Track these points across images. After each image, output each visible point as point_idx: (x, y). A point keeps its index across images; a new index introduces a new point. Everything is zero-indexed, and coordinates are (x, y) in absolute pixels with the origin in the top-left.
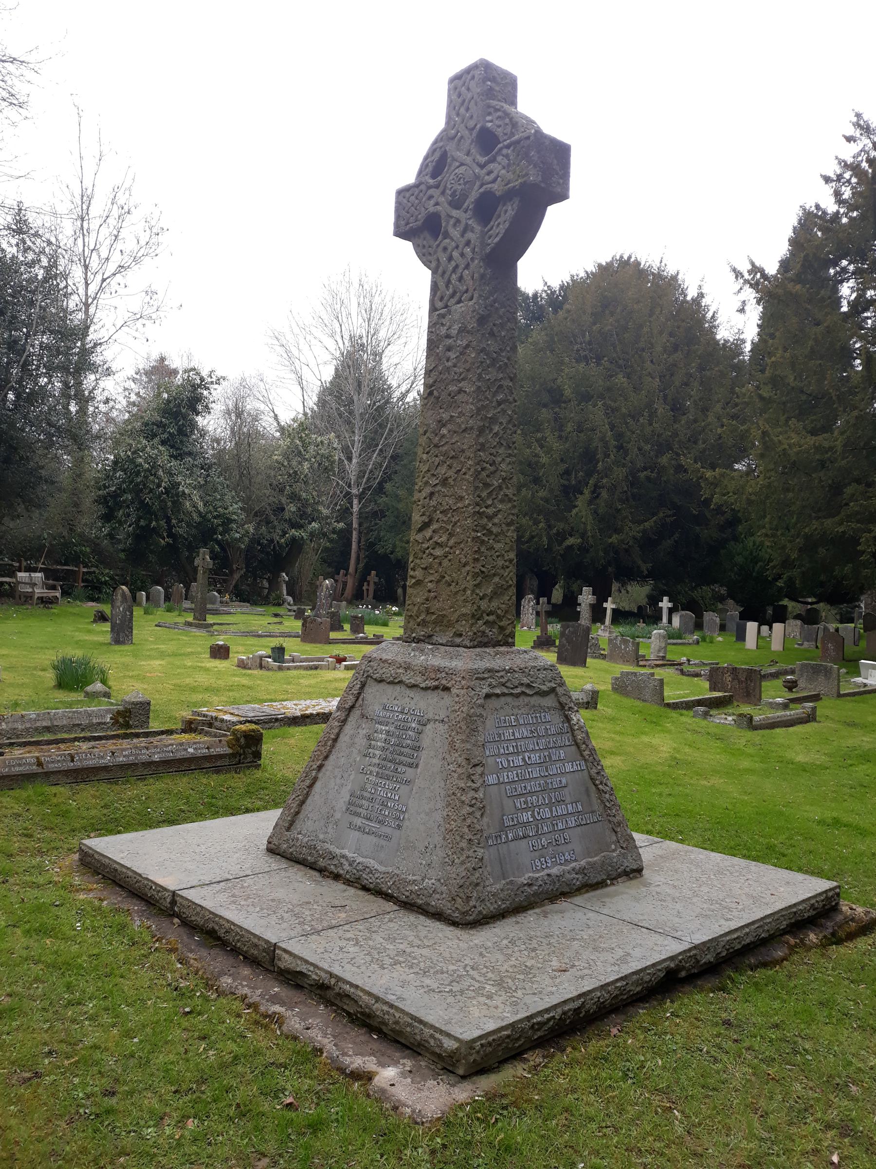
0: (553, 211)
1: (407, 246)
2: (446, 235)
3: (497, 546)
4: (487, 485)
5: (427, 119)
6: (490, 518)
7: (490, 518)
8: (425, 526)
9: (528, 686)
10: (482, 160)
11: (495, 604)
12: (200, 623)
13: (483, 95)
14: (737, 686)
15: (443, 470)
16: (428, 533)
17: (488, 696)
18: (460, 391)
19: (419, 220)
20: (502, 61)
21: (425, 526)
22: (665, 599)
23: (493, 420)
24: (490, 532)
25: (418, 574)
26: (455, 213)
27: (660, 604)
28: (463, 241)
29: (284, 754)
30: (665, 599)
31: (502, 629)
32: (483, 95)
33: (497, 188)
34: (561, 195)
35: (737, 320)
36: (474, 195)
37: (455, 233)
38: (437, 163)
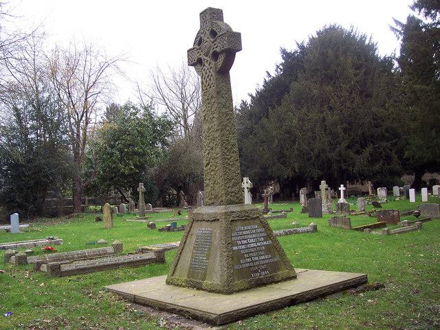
0: (238, 54)
1: (235, 30)
2: (204, 66)
3: (232, 169)
4: (226, 148)
5: (193, 27)
6: (229, 159)
7: (229, 159)
8: (208, 164)
9: (248, 216)
10: (212, 40)
11: (234, 189)
12: (143, 215)
13: (212, 17)
14: (386, 219)
15: (211, 144)
16: (209, 167)
17: (232, 221)
18: (214, 117)
19: (196, 61)
20: (215, 6)
21: (208, 164)
22: (342, 186)
23: (227, 126)
24: (229, 164)
25: (207, 182)
26: (205, 58)
27: (340, 189)
28: (210, 67)
29: (170, 258)
30: (342, 186)
31: (238, 198)
32: (212, 17)
33: (218, 50)
34: (240, 49)
35: (389, 46)
36: (211, 52)
37: (207, 65)
38: (199, 41)
